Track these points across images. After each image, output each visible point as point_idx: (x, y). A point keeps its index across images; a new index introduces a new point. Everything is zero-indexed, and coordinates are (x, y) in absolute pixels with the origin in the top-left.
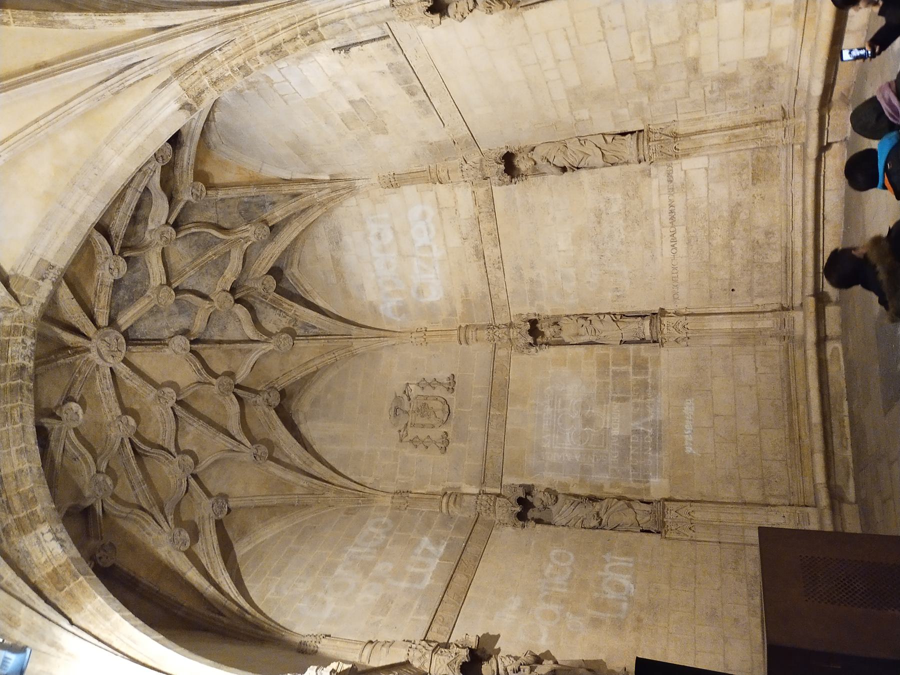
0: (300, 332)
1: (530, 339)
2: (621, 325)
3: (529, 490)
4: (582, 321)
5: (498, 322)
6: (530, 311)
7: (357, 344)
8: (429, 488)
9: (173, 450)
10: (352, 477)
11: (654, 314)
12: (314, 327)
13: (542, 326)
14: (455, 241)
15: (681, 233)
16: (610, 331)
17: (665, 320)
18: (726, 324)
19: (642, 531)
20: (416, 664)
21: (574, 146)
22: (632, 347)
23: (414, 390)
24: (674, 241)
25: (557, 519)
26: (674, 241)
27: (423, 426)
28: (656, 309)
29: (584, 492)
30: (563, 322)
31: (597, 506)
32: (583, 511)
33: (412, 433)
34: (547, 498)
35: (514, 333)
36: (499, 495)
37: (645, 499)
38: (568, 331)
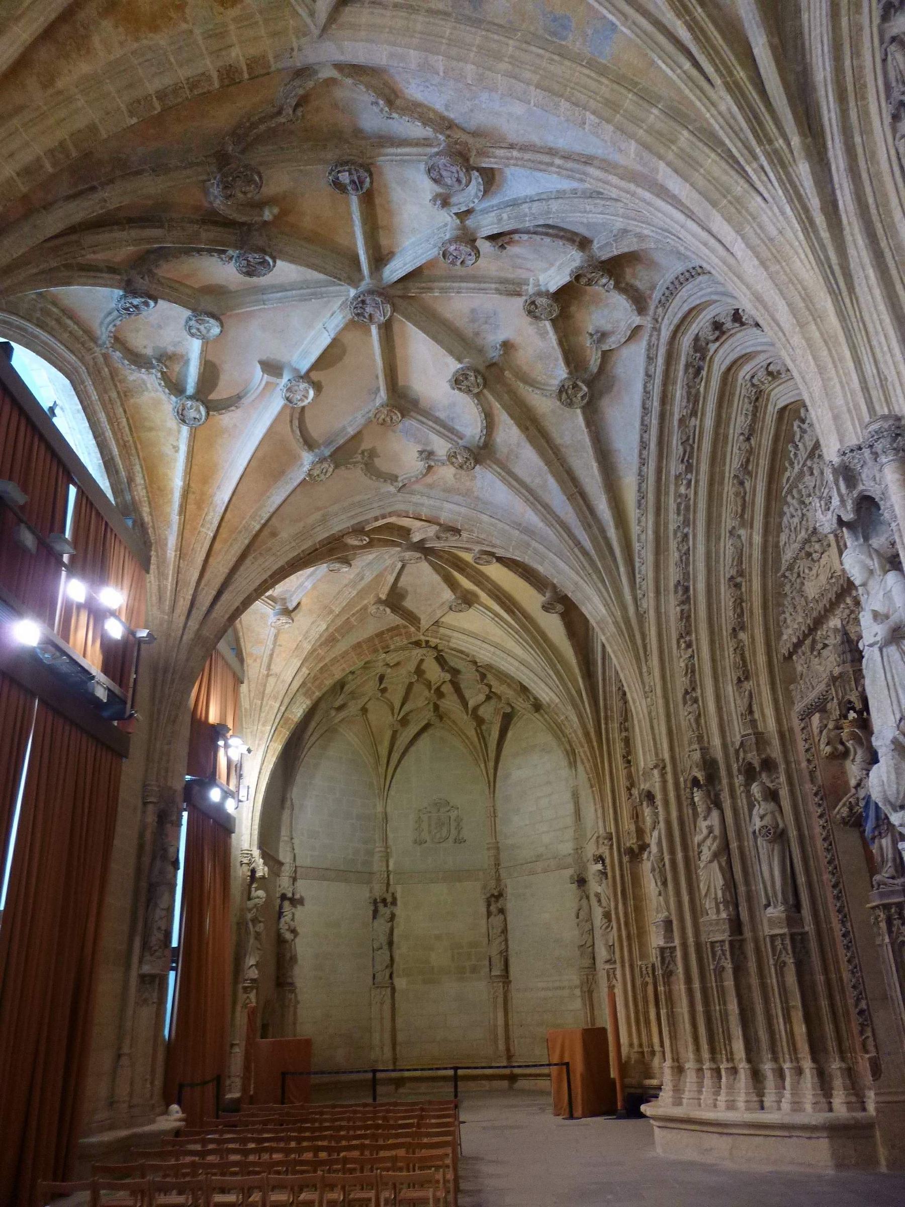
0: (484, 727)
1: (488, 895)
2: (498, 956)
3: (394, 902)
4: (500, 930)
5: (501, 871)
6: (509, 891)
7: (482, 766)
8: (391, 835)
9: (382, 686)
10: (394, 780)
11: (508, 977)
12: (490, 735)
13: (501, 901)
14: (546, 839)
15: (550, 994)
16: (494, 951)
17: (501, 984)
18: (501, 1022)
19: (374, 975)
20: (283, 868)
21: (587, 926)
22: (487, 963)
23: (453, 814)
24: (548, 989)
25: (376, 923)
26: (548, 989)
27: (429, 825)
28: (511, 978)
29: (395, 939)
30: (501, 917)
31: (386, 947)
32: (383, 939)
33: (425, 818)
34: (388, 915)
35: (493, 883)
36: (388, 884)
37: (394, 975)
38: (497, 920)
